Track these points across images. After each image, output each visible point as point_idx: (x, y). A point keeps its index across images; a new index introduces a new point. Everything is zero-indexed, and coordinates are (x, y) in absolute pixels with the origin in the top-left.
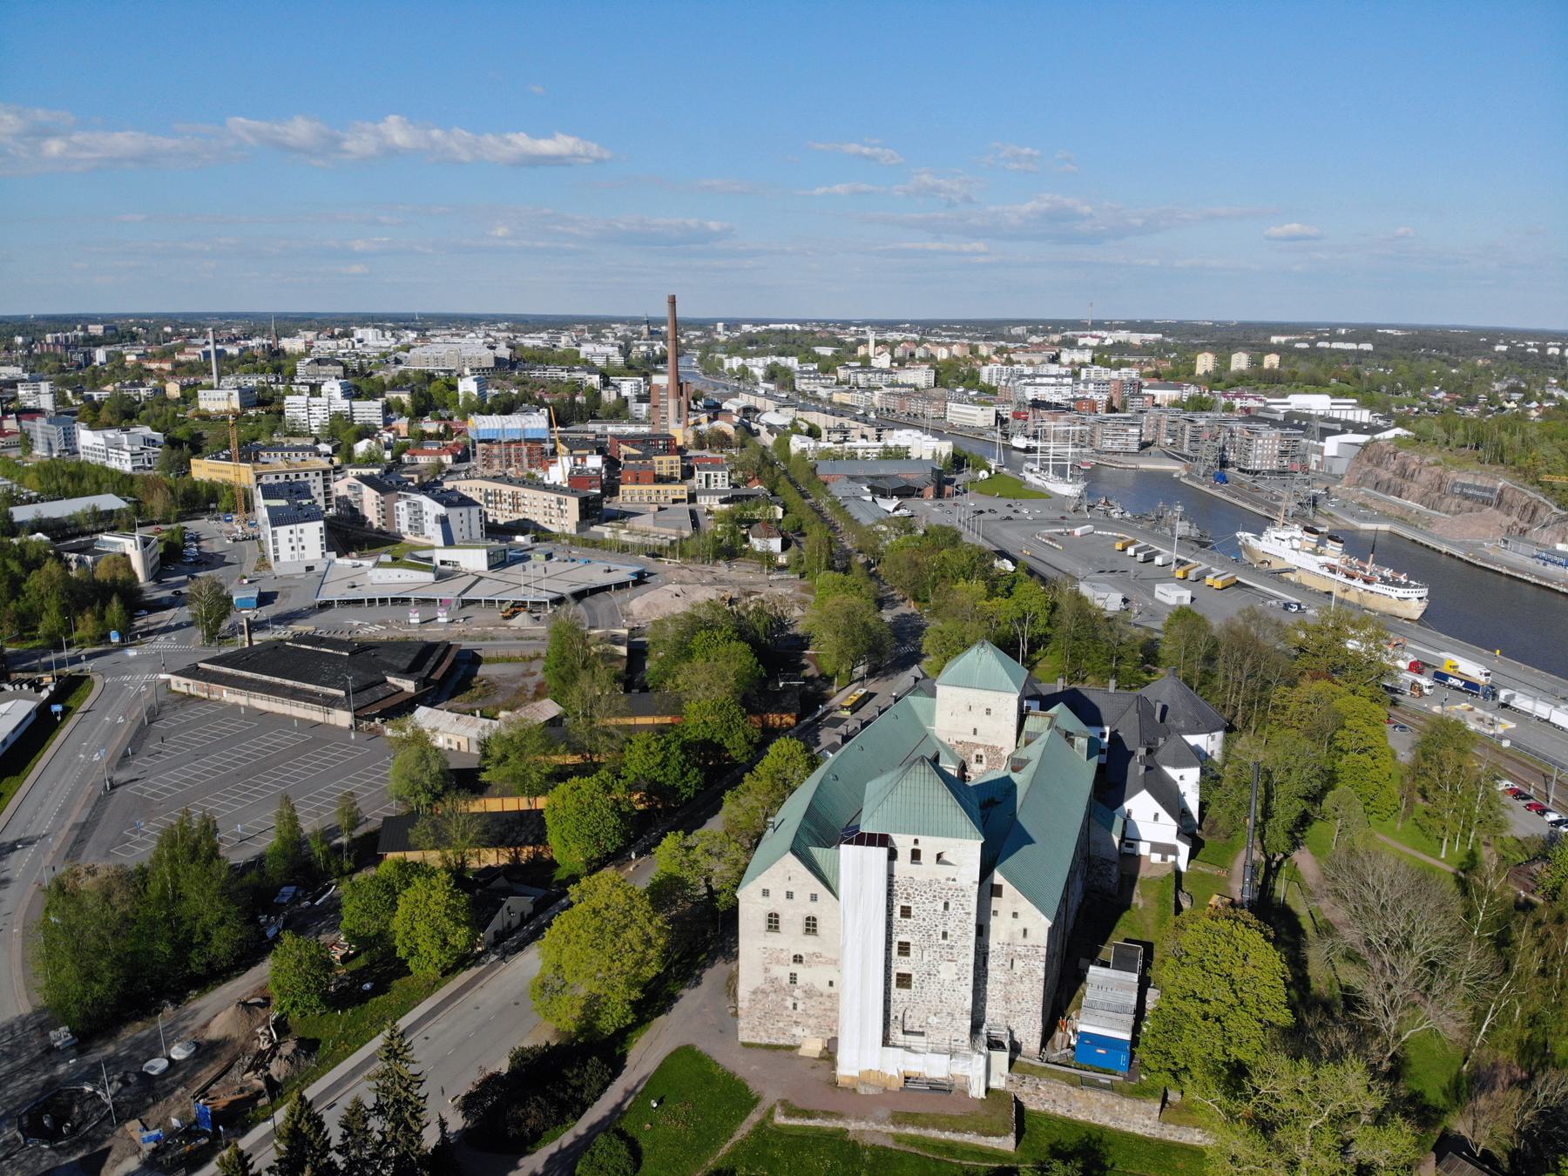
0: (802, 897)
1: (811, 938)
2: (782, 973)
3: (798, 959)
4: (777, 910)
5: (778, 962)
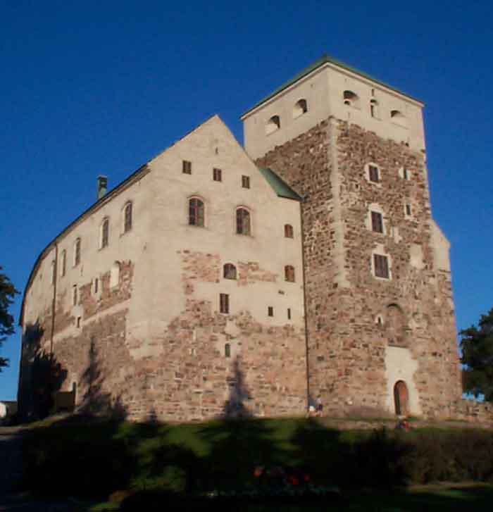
0: (232, 177)
1: (243, 239)
2: (208, 292)
3: (229, 270)
4: (203, 193)
5: (205, 275)
